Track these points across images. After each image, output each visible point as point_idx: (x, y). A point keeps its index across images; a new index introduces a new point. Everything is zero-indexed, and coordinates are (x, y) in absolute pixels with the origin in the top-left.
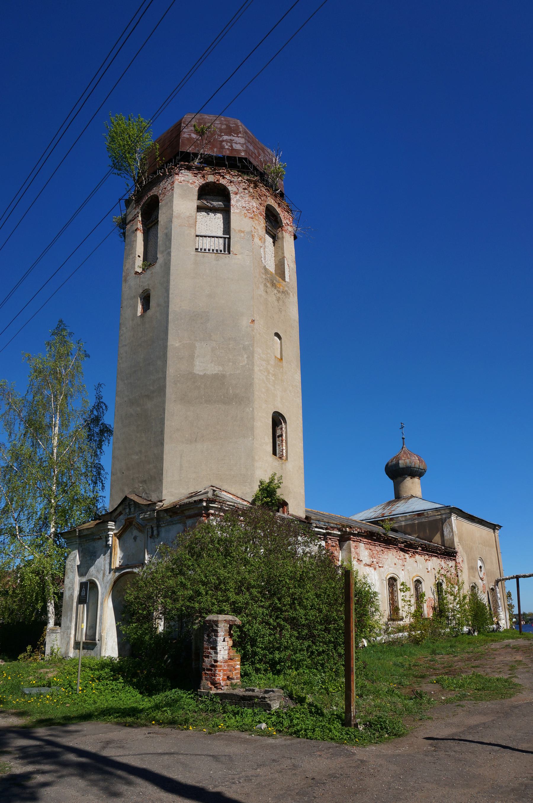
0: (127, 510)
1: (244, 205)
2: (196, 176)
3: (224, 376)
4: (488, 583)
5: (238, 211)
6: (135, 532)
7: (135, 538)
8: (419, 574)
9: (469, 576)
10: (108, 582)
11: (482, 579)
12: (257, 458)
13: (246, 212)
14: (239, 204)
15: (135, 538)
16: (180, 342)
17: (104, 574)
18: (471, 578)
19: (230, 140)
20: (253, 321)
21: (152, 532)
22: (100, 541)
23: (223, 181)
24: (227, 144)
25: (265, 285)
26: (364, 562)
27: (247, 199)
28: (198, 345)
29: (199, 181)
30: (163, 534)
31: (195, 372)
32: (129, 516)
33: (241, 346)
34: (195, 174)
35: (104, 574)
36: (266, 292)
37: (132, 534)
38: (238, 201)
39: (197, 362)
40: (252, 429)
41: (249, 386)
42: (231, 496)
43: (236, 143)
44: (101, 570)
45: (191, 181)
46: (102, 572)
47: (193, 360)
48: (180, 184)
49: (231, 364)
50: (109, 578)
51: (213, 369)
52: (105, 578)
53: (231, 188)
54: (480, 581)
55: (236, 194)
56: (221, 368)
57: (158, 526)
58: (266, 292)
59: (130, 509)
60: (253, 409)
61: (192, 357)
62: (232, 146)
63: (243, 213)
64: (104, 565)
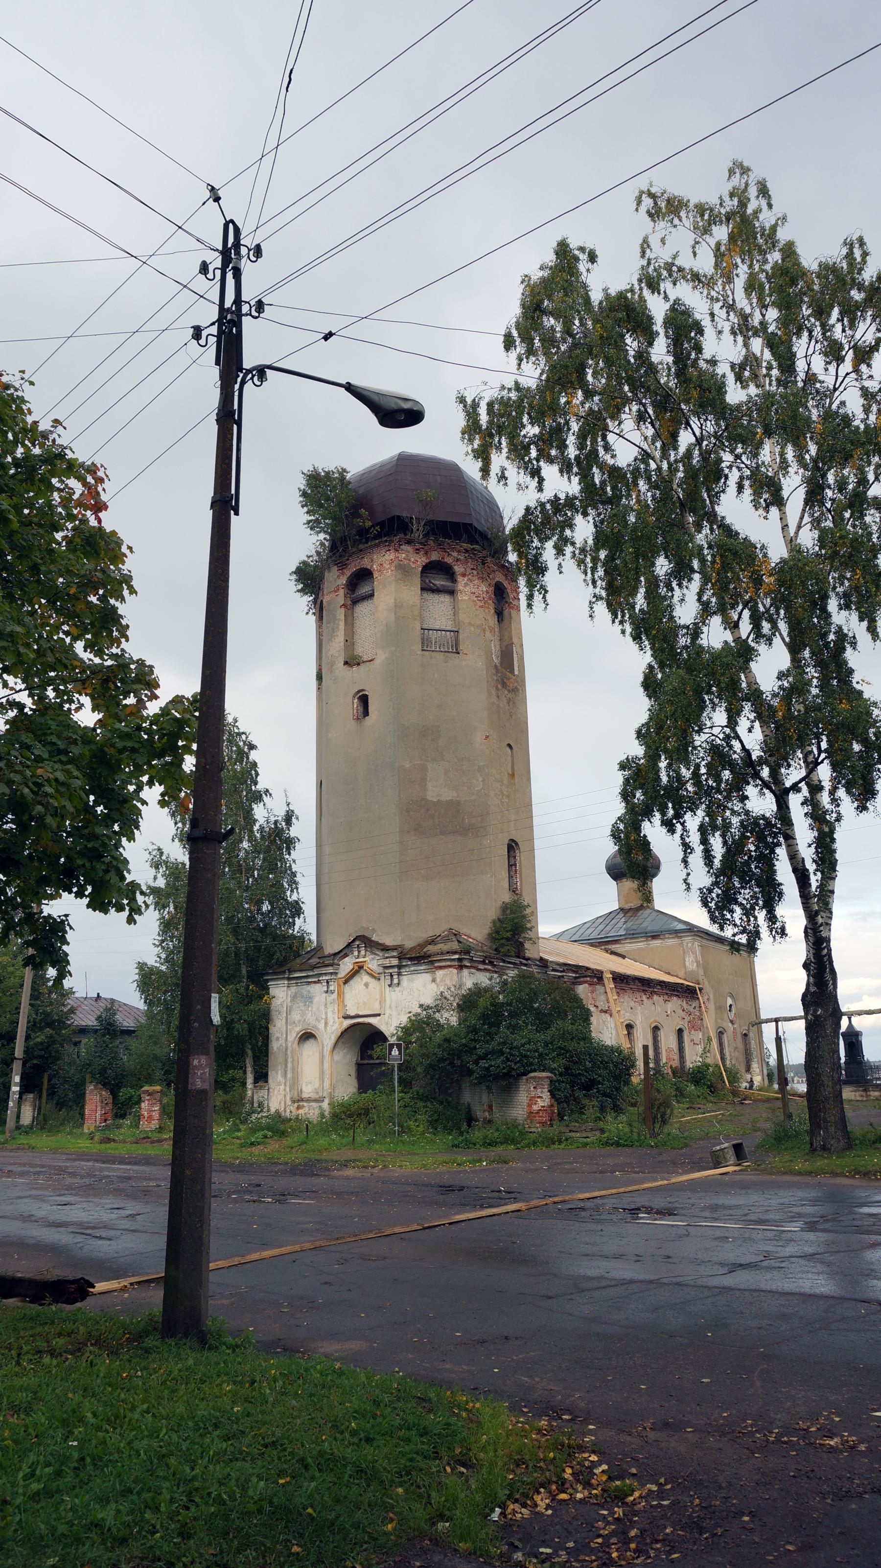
0: (356, 953)
3: (458, 803)
4: (740, 1027)
6: (366, 978)
7: (366, 985)
8: (657, 1019)
9: (716, 1019)
10: (332, 1033)
11: (732, 1022)
17: (326, 1024)
18: (719, 1020)
21: (392, 980)
22: (318, 985)
23: (449, 560)
26: (600, 1008)
28: (429, 765)
30: (405, 980)
32: (357, 960)
35: (326, 1024)
39: (429, 787)
46: (323, 1021)
50: (334, 1028)
51: (449, 795)
52: (328, 1028)
54: (730, 1024)
56: (455, 794)
57: (399, 974)
59: (359, 952)
61: (424, 780)
64: (326, 1013)
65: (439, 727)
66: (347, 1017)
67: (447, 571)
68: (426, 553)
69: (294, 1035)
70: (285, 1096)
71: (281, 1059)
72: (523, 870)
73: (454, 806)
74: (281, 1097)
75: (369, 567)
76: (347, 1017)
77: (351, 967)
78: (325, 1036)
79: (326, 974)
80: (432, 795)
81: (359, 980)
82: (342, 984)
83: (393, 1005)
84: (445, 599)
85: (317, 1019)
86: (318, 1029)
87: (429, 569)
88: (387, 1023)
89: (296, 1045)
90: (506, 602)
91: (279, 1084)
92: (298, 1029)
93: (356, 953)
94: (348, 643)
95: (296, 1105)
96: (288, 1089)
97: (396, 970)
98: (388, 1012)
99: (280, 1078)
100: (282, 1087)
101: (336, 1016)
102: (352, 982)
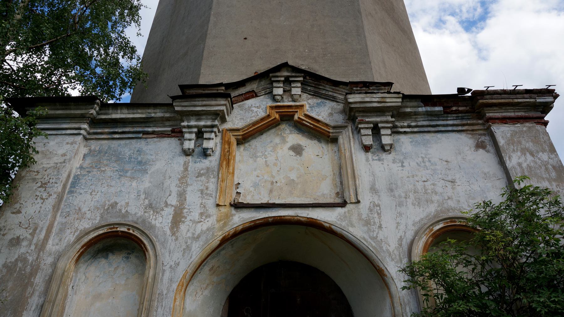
15: (297, 150)
37: (284, 141)
44: (167, 205)
52: (183, 227)
64: (182, 195)
66: (238, 206)
69: (69, 237)
76: (238, 206)
77: (262, 114)
78: (171, 244)
79: (198, 115)
81: (277, 140)
82: (233, 140)
83: (381, 185)
85: (150, 206)
86: (152, 227)
88: (367, 223)
89: (67, 263)
93: (279, 91)
98: (366, 198)
101: (210, 203)
102: (256, 143)
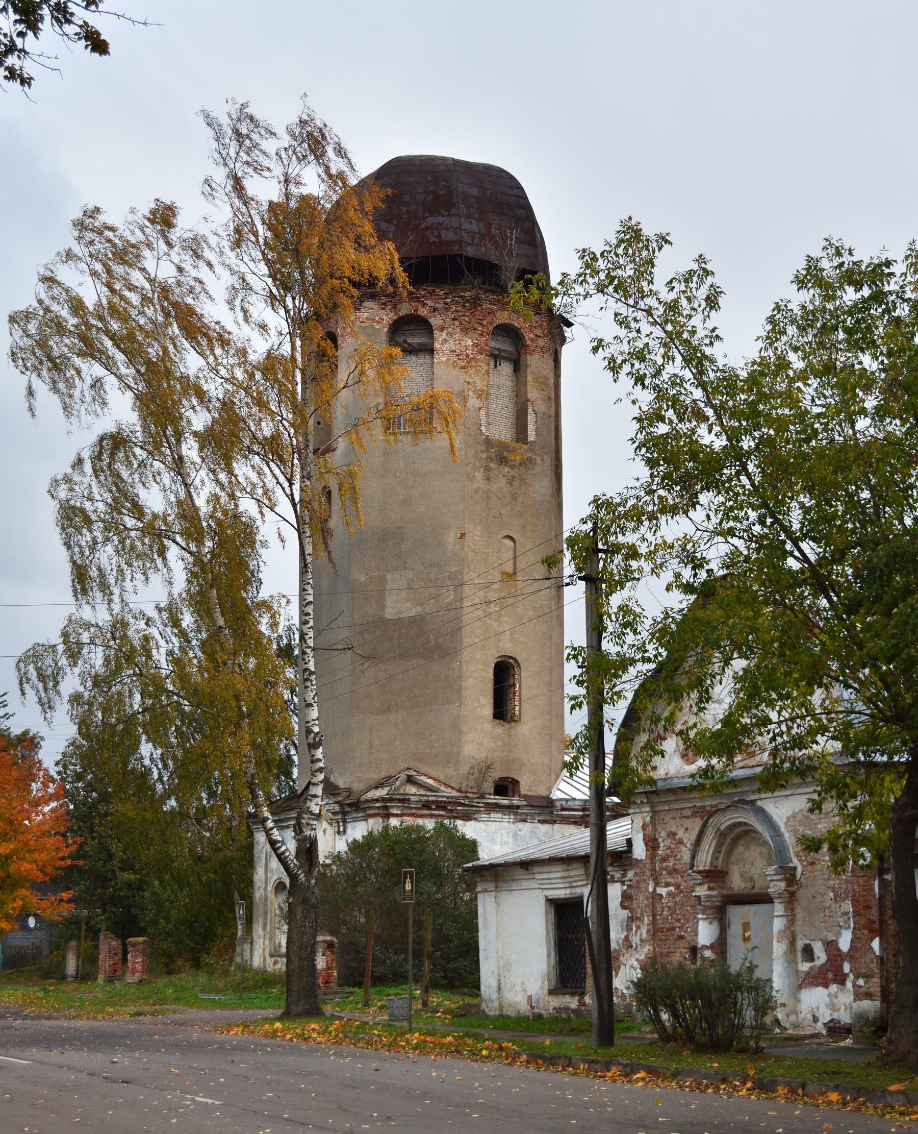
1: (453, 348)
2: (384, 309)
5: (444, 359)
12: (465, 729)
13: (456, 359)
14: (446, 347)
16: (366, 574)
19: (438, 223)
20: (463, 535)
23: (423, 312)
24: (432, 233)
25: (487, 469)
27: (457, 335)
28: (389, 577)
29: (388, 317)
31: (386, 616)
33: (446, 574)
34: (383, 304)
36: (489, 479)
38: (445, 341)
39: (389, 603)
40: (459, 691)
41: (456, 632)
42: (431, 782)
43: (447, 229)
45: (377, 318)
47: (384, 600)
48: (363, 325)
49: (432, 601)
51: (410, 610)
53: (435, 321)
55: (442, 329)
56: (419, 609)
58: (489, 479)
60: (461, 664)
61: (382, 594)
62: (439, 236)
63: (451, 362)
65: (403, 527)
67: (424, 326)
68: (395, 307)
70: (264, 950)
71: (261, 910)
72: (523, 692)
73: (418, 622)
74: (261, 951)
75: (334, 331)
80: (390, 612)
84: (423, 359)
87: (397, 328)
90: (523, 345)
91: (260, 938)
92: (275, 878)
94: (321, 426)
95: (273, 959)
96: (267, 942)
97: (340, 816)
99: (260, 931)
100: (262, 940)
